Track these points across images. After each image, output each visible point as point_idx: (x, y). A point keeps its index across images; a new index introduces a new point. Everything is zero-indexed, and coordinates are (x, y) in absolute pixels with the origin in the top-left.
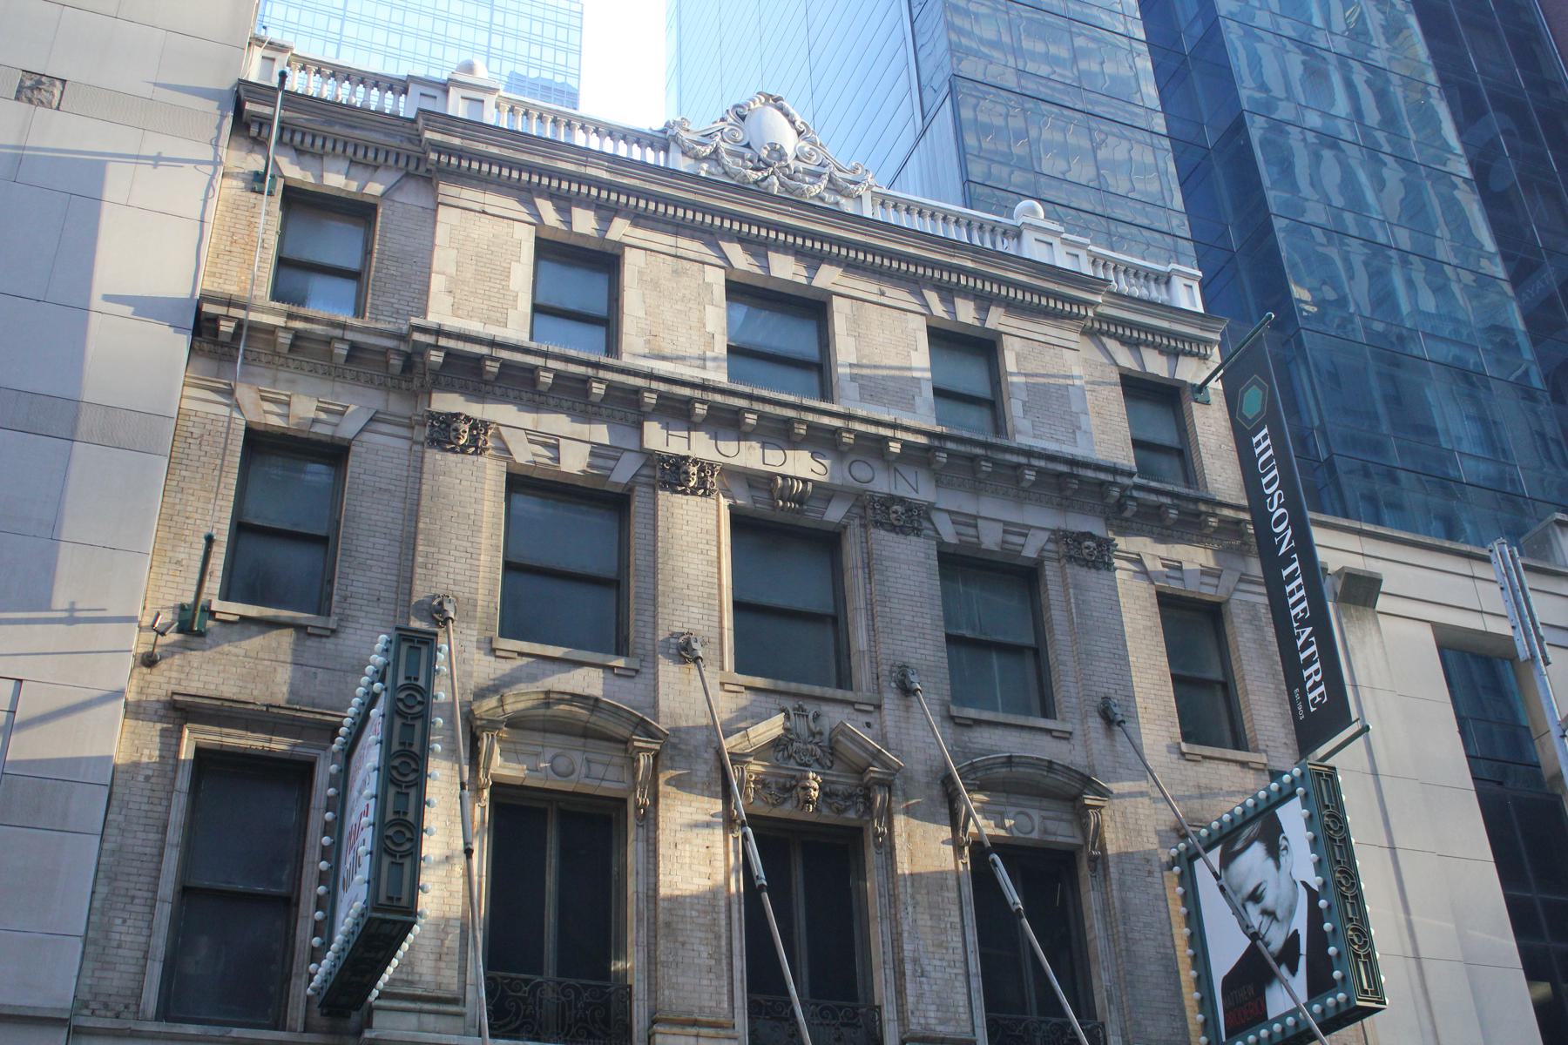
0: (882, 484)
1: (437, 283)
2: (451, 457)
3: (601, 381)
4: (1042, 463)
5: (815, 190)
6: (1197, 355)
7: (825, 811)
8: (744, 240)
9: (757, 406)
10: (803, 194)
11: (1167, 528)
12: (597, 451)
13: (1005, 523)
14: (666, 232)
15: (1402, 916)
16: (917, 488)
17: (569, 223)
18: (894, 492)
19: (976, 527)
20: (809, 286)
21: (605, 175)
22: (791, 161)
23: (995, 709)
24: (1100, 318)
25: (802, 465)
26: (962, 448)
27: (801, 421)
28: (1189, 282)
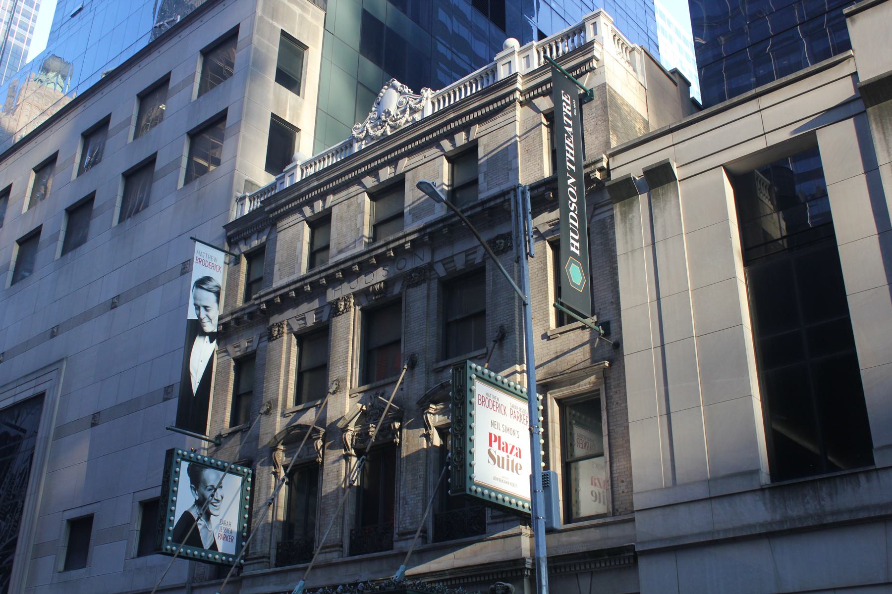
0: (409, 265)
1: (276, 267)
2: (274, 342)
3: (306, 285)
4: (469, 213)
5: (404, 120)
6: (587, 72)
7: (381, 439)
8: (369, 173)
9: (356, 261)
10: (399, 126)
11: (552, 202)
12: (318, 312)
13: (466, 251)
14: (344, 189)
15: (662, 388)
16: (423, 259)
17: (313, 211)
18: (414, 266)
19: (453, 261)
20: (396, 176)
21: (316, 183)
22: (392, 113)
23: (470, 352)
24: (529, 90)
25: (379, 275)
26: (433, 228)
27: (371, 257)
28: (593, 21)
